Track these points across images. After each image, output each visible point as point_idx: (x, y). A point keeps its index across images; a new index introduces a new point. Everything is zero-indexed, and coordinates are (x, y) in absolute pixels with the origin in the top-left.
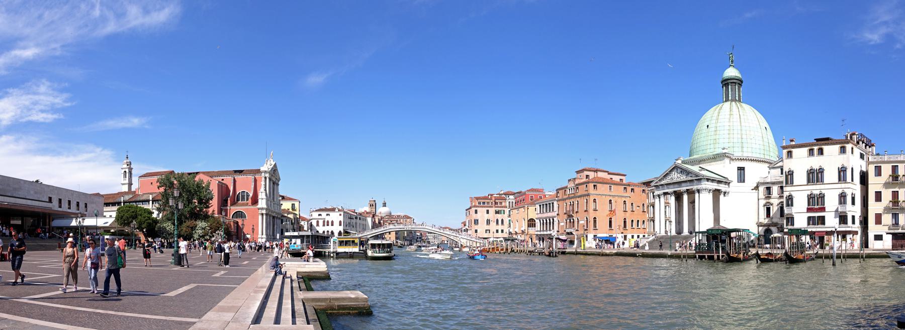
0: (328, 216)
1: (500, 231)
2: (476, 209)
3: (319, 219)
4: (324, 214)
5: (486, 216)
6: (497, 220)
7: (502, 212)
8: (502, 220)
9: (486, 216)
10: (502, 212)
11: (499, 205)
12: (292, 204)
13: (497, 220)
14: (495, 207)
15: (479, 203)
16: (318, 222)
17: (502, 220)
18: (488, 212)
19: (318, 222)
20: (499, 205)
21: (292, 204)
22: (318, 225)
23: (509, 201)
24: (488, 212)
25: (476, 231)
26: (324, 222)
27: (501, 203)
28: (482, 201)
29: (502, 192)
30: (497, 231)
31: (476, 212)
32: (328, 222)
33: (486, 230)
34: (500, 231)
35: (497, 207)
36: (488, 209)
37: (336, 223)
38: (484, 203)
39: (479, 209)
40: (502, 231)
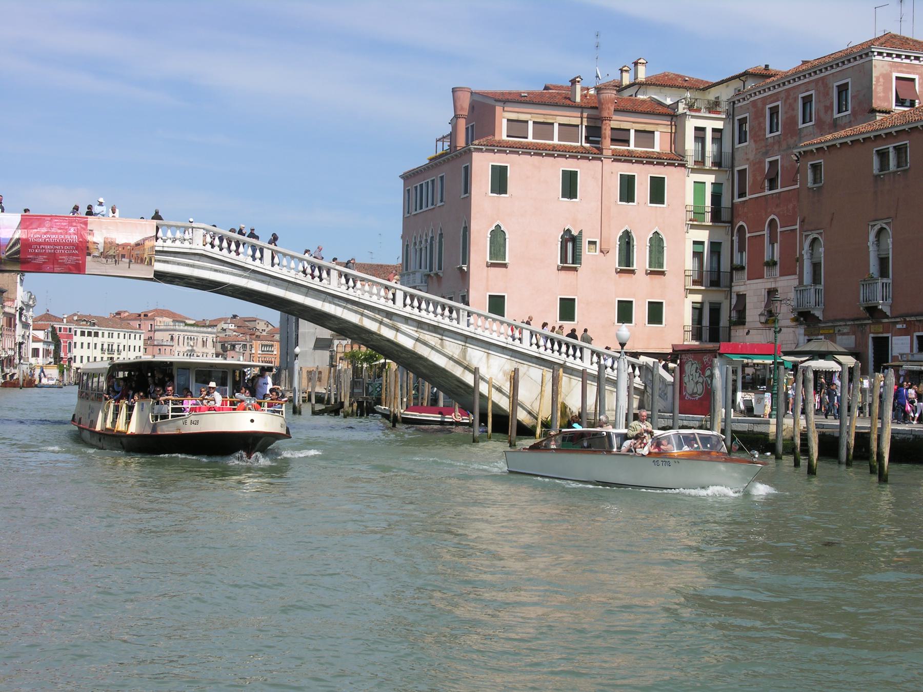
1: (640, 312)
2: (499, 160)
6: (627, 241)
8: (657, 243)
11: (632, 147)
13: (627, 241)
14: (618, 158)
15: (517, 126)
17: (657, 243)
18: (570, 185)
20: (632, 147)
23: (701, 123)
24: (570, 185)
25: (497, 304)
27: (646, 136)
28: (530, 116)
29: (642, 74)
30: (625, 312)
31: (500, 180)
34: (640, 312)
35: (628, 158)
36: (570, 165)
38: (543, 128)
39: (516, 165)
40: (655, 313)
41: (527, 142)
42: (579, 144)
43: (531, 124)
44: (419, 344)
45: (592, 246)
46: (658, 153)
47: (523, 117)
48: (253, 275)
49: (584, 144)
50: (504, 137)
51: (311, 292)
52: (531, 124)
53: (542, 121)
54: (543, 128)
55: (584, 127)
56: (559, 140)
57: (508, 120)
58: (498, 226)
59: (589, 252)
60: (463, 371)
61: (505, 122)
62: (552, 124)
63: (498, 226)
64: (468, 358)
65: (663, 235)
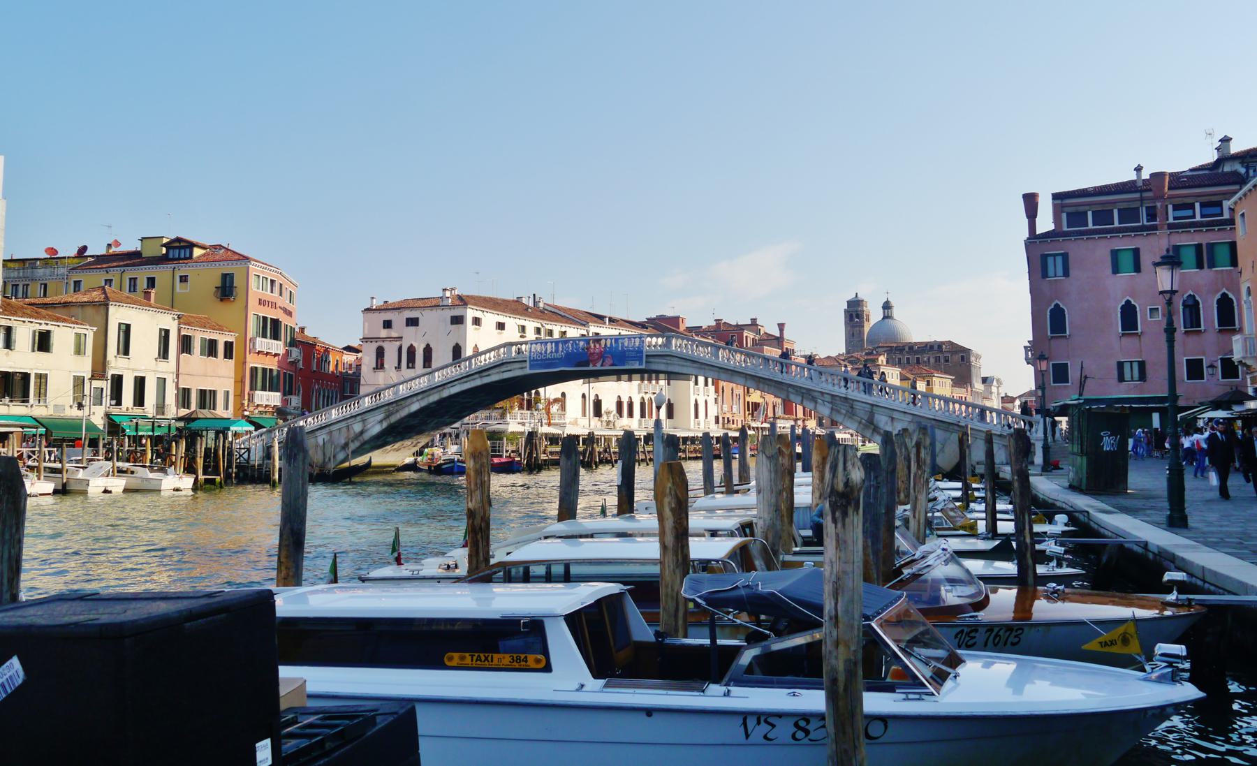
0: (412, 329)
3: (384, 339)
4: (398, 319)
5: (1120, 287)
7: (1223, 254)
9: (1120, 287)
10: (1223, 254)
12: (225, 276)
16: (380, 353)
19: (380, 353)
21: (225, 276)
22: (380, 366)
26: (400, 349)
32: (412, 351)
33: (1120, 365)
37: (442, 356)
41: (1114, 228)
42: (1141, 224)
43: (1090, 214)
44: (834, 413)
45: (1155, 313)
46: (1226, 220)
47: (1082, 209)
48: (707, 367)
49: (1145, 223)
50: (1065, 229)
51: (747, 377)
52: (1090, 214)
53: (1100, 209)
54: (1103, 216)
55: (1144, 209)
56: (1120, 223)
57: (1068, 215)
58: (1057, 305)
59: (1151, 318)
60: (873, 433)
61: (1064, 215)
62: (1112, 211)
63: (1057, 305)
64: (875, 423)
65: (1231, 296)
